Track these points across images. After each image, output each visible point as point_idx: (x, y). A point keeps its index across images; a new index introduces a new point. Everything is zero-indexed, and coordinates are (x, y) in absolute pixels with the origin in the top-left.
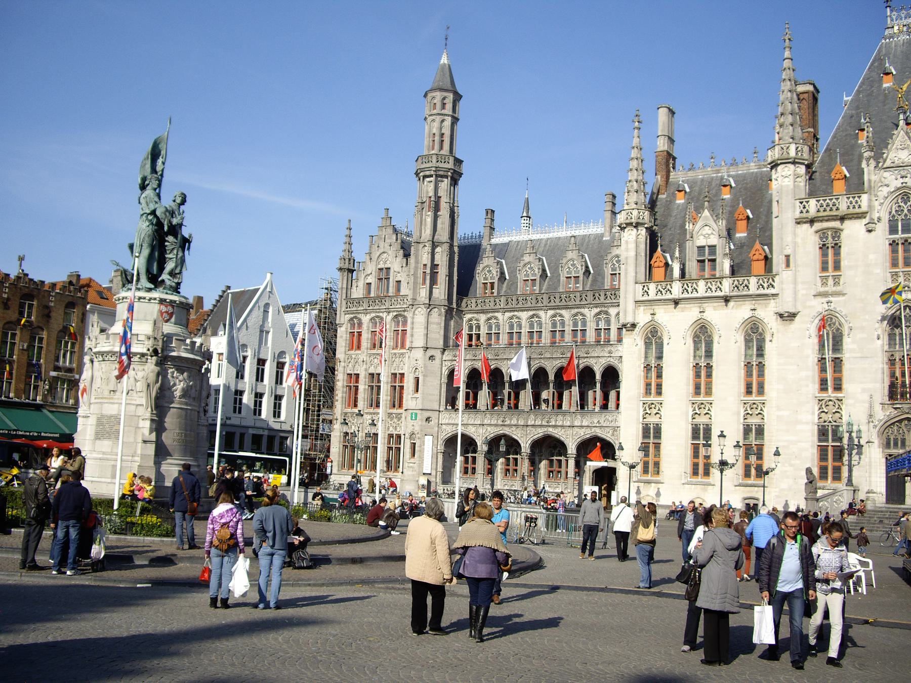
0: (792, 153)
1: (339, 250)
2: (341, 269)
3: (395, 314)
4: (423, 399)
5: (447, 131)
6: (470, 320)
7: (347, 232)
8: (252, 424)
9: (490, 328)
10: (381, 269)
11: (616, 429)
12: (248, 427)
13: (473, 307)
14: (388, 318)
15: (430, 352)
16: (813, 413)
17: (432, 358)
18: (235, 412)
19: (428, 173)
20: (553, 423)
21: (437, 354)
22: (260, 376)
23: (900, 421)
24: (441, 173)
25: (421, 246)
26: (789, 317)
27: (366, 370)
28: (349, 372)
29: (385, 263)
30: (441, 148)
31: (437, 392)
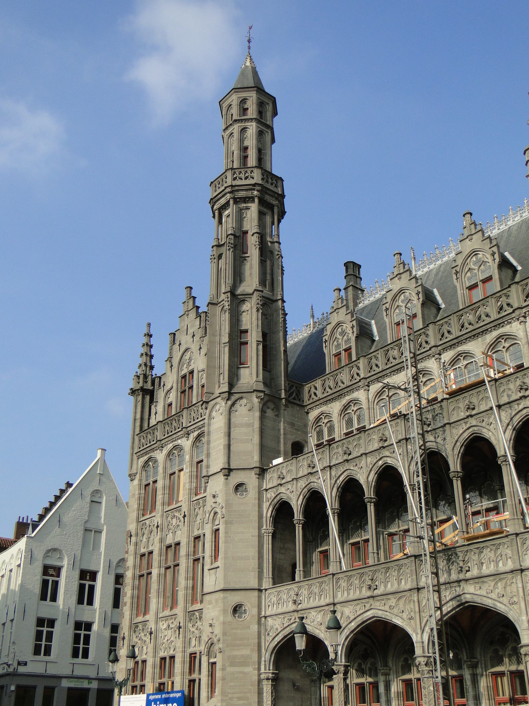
2: (133, 392)
3: (196, 433)
4: (226, 569)
5: (251, 141)
6: (318, 419)
7: (145, 340)
8: (67, 672)
9: (349, 422)
10: (184, 377)
12: (59, 678)
13: (320, 395)
14: (186, 443)
15: (236, 478)
18: (37, 651)
19: (223, 201)
20: (475, 572)
22: (85, 596)
24: (242, 194)
25: (218, 309)
27: (161, 540)
28: (143, 551)
29: (189, 365)
31: (253, 552)
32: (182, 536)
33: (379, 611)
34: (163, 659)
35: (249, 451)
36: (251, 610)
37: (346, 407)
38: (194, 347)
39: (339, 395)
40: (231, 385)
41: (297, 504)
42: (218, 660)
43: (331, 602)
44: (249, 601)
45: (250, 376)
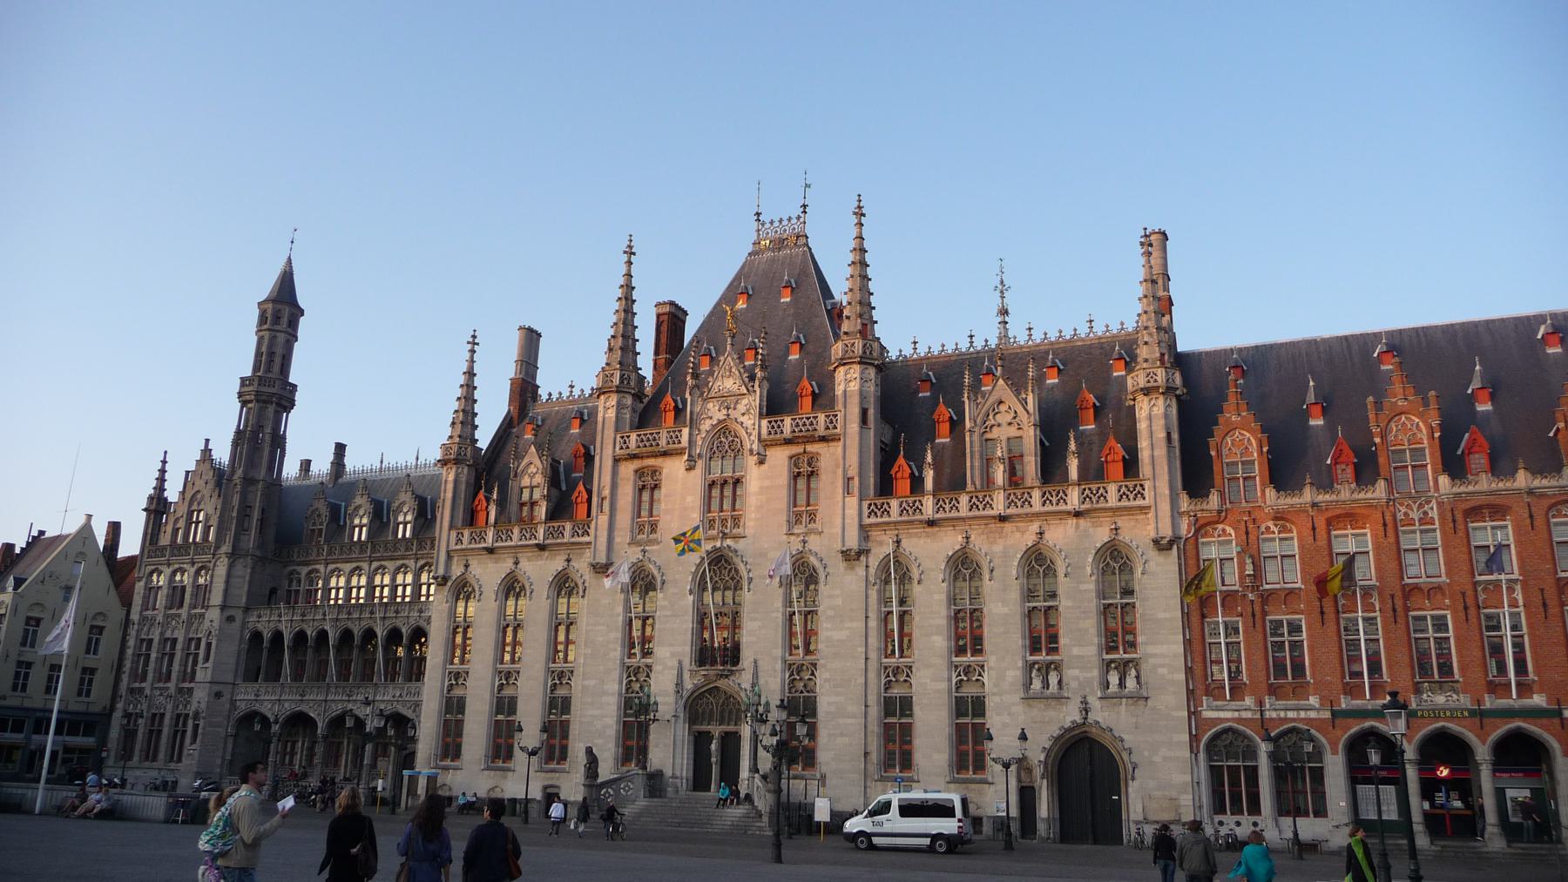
0: (616, 381)
1: (149, 489)
6: (291, 573)
11: (418, 705)
16: (621, 682)
17: (230, 619)
18: (15, 688)
21: (239, 615)
23: (710, 691)
26: (602, 569)
27: (162, 634)
30: (268, 370)
31: (233, 661)
32: (180, 635)
33: (304, 708)
34: (154, 715)
35: (241, 596)
36: (227, 696)
37: (310, 572)
38: (206, 492)
39: (307, 564)
40: (234, 547)
41: (267, 635)
42: (201, 723)
43: (276, 701)
44: (226, 691)
45: (250, 541)
